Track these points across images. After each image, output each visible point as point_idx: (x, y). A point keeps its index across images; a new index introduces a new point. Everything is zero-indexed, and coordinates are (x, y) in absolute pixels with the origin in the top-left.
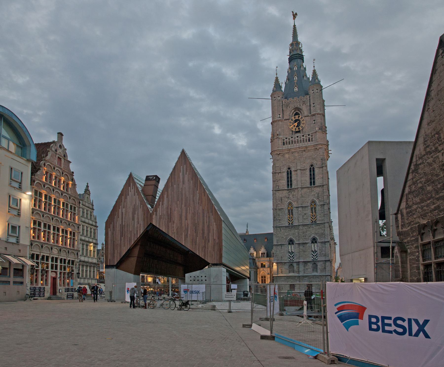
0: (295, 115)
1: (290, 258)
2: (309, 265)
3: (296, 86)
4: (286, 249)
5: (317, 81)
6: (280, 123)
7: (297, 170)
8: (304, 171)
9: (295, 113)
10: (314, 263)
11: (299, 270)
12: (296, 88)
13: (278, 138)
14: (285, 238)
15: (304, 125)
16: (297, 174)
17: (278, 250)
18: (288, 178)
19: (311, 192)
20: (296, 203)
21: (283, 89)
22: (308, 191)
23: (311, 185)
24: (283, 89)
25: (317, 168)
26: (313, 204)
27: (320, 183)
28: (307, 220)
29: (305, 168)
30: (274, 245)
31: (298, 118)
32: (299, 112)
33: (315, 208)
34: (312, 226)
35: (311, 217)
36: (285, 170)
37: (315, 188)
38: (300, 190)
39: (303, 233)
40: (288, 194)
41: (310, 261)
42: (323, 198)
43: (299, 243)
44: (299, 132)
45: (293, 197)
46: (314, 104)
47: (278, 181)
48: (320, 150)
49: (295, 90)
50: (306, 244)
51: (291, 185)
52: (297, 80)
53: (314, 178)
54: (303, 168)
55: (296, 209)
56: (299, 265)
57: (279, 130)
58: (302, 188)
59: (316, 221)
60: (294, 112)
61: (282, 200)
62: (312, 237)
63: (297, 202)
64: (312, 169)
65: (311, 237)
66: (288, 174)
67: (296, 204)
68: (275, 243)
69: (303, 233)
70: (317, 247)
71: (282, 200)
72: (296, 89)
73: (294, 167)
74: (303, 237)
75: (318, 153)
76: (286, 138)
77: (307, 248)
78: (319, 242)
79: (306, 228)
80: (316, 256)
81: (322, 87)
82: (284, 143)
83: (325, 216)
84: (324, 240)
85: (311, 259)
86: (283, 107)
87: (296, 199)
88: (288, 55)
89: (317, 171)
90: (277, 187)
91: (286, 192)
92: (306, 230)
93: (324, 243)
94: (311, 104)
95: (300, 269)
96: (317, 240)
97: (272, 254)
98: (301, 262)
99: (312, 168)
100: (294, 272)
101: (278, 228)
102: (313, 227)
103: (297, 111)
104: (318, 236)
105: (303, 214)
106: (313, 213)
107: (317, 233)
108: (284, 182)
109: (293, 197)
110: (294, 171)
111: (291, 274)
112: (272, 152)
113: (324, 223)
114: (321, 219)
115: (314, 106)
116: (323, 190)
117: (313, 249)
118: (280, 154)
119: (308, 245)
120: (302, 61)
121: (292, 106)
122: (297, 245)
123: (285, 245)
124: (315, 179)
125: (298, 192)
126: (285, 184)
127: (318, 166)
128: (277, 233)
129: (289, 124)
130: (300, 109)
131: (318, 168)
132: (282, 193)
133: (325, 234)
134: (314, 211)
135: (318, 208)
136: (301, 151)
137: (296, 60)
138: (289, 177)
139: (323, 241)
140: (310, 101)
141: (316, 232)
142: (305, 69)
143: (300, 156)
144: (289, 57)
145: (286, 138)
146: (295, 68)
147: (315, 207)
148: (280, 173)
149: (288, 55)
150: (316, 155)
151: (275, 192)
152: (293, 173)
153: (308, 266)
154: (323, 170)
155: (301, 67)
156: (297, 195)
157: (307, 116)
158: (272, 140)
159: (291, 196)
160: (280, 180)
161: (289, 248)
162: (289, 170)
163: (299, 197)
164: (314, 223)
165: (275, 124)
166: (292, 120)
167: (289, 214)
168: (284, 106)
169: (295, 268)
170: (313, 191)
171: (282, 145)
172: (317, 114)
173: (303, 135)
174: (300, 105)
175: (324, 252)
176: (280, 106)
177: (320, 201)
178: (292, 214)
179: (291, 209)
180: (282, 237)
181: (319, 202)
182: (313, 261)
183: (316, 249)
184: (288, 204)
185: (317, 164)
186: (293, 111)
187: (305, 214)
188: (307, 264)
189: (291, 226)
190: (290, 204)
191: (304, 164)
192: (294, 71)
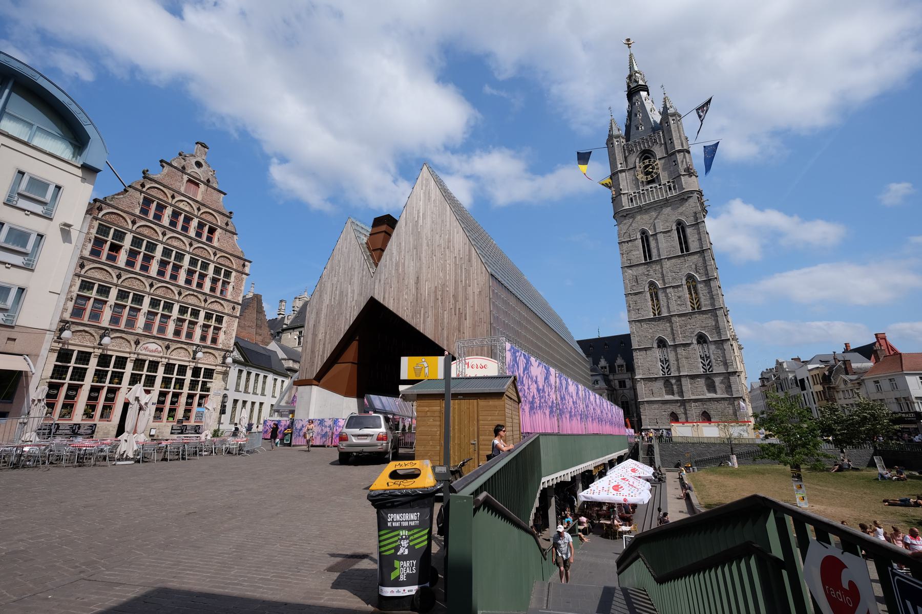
0: (644, 159)
9: (643, 157)
22: (679, 261)
23: (682, 251)
31: (649, 162)
32: (650, 155)
39: (681, 328)
44: (652, 181)
45: (656, 274)
62: (697, 334)
63: (664, 280)
80: (708, 365)
87: (660, 275)
89: (689, 231)
93: (720, 342)
96: (706, 338)
98: (684, 375)
102: (696, 317)
103: (646, 155)
108: (638, 254)
110: (652, 235)
118: (628, 216)
119: (692, 346)
122: (672, 347)
135: (700, 287)
141: (704, 325)
145: (634, 193)
147: (695, 285)
148: (630, 241)
152: (651, 239)
159: (652, 272)
162: (644, 236)
164: (697, 310)
179: (654, 292)
181: (699, 277)
186: (640, 155)
187: (679, 297)
189: (658, 318)
190: (652, 284)
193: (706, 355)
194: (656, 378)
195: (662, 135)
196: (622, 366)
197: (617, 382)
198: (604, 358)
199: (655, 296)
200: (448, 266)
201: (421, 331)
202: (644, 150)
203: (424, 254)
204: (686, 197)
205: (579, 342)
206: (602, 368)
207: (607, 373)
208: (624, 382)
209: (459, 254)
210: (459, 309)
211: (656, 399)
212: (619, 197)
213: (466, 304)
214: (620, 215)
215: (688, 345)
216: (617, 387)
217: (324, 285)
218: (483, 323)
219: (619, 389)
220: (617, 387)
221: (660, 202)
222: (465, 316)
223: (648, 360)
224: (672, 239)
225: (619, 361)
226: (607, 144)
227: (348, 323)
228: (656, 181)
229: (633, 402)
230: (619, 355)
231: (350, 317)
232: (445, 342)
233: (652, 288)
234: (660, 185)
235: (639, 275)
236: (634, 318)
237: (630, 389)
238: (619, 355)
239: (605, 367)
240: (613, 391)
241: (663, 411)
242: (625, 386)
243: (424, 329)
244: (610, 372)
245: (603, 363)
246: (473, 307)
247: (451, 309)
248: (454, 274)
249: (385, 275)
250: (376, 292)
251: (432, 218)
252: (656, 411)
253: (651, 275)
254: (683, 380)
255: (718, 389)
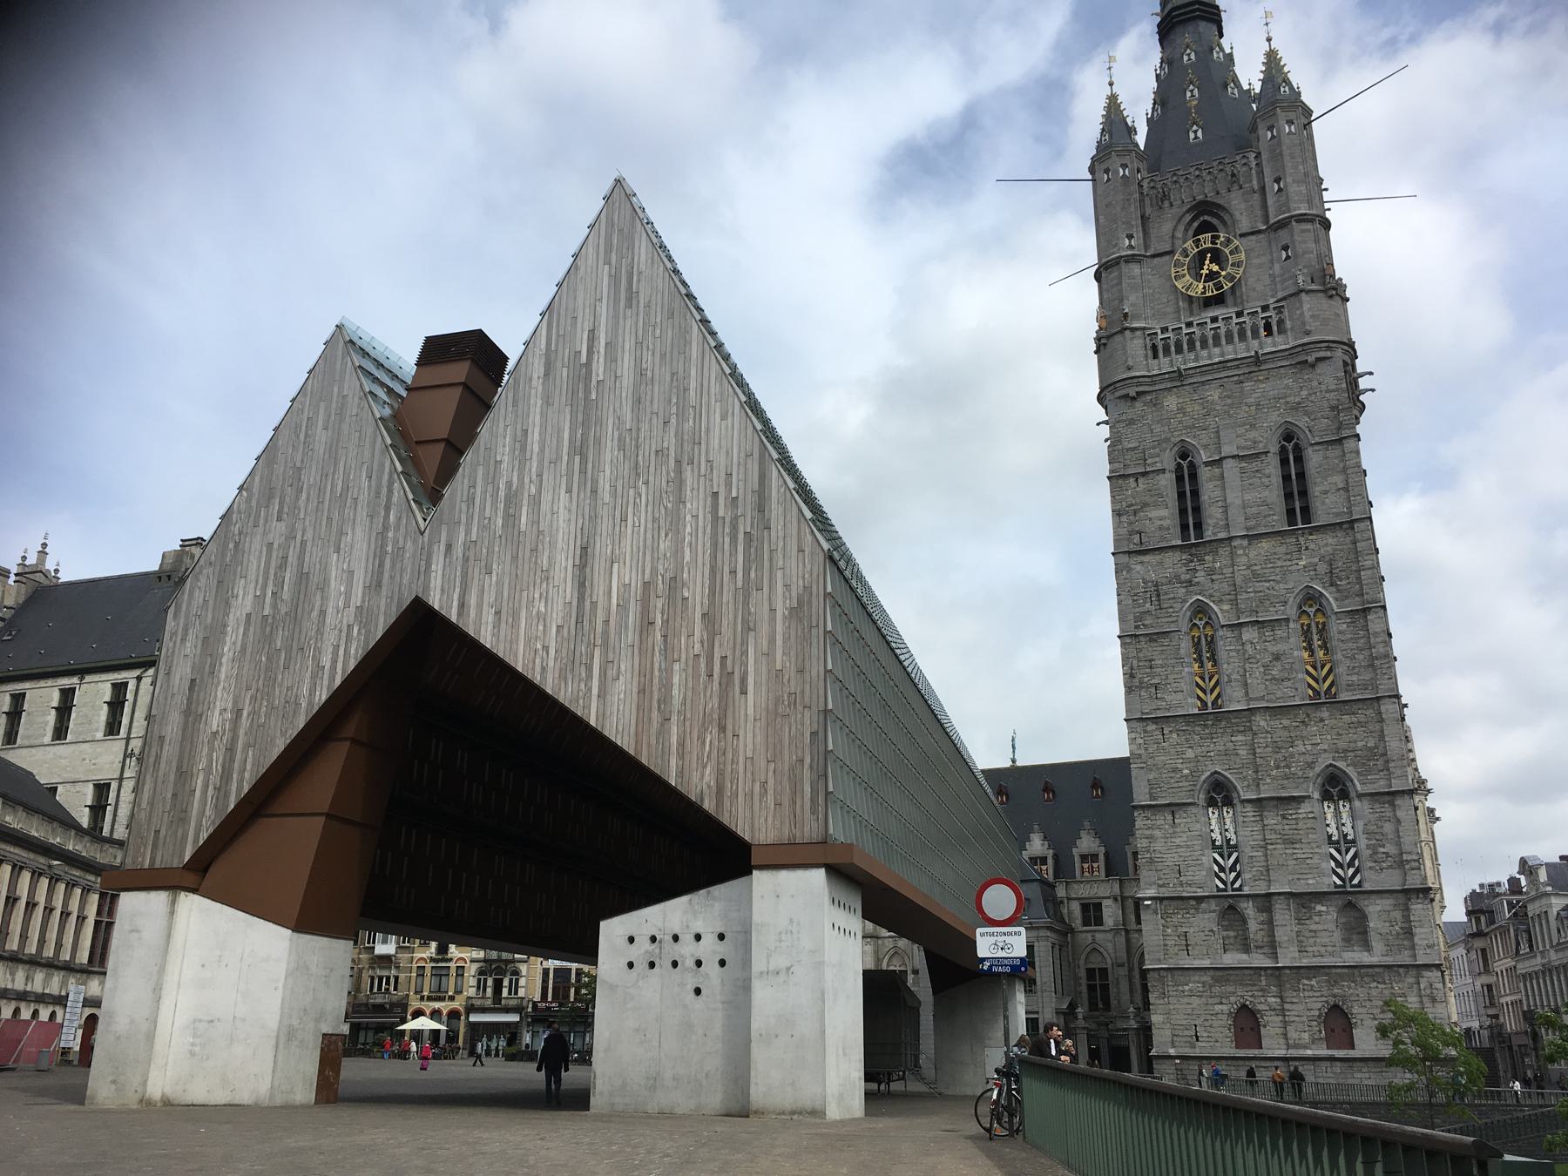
0: (1197, 233)
1: (1222, 875)
2: (1320, 914)
3: (1194, 123)
4: (1198, 826)
5: (1287, 89)
6: (1135, 269)
7: (1221, 459)
8: (1256, 465)
9: (1196, 224)
10: (1349, 901)
11: (1272, 934)
12: (1195, 128)
13: (1126, 329)
14: (1186, 771)
15: (1242, 270)
16: (1222, 477)
17: (1157, 833)
18: (1181, 495)
19: (1295, 555)
20: (1226, 607)
21: (1141, 139)
22: (1283, 549)
23: (1292, 521)
24: (1141, 139)
25: (1312, 445)
26: (1311, 611)
27: (1337, 515)
28: (1289, 684)
29: (1260, 448)
30: (1135, 807)
31: (1213, 243)
32: (1215, 221)
33: (1323, 630)
34: (1318, 714)
35: (1308, 673)
36: (1168, 460)
37: (1311, 534)
38: (1244, 549)
39: (1278, 749)
40: (1185, 565)
41: (1325, 893)
42: (1359, 578)
43: (1260, 800)
44: (1219, 300)
46: (1278, 180)
47: (1135, 512)
48: (1321, 368)
49: (1192, 136)
50: (1294, 805)
51: (1199, 526)
52: (1200, 100)
53: (1304, 493)
54: (1249, 448)
55: (1229, 634)
56: (1268, 910)
57: (1132, 298)
58: (1253, 538)
59: (1333, 690)
60: (1193, 220)
61: (1158, 595)
62: (1323, 770)
63: (1234, 603)
64: (1291, 451)
65: (1318, 769)
66: (1180, 479)
67: (1227, 611)
68: (1141, 796)
69: (1278, 749)
70: (1353, 818)
71: (1158, 595)
72: (1196, 134)
73: (1206, 447)
74: (1278, 767)
75: (1315, 383)
76: (1165, 330)
77: (1301, 825)
78: (1360, 796)
79: (1286, 722)
80: (1351, 864)
81: (1308, 112)
82: (1154, 348)
83: (1377, 663)
84: (1382, 782)
85: (1326, 881)
86: (1142, 207)
87: (1226, 587)
88: (1157, 14)
89: (1314, 459)
90: (1136, 538)
91: (1177, 556)
92: (1287, 734)
93: (1387, 798)
94: (1268, 180)
95: (1281, 934)
96: (1348, 784)
97: (1129, 855)
98: (1280, 894)
99: (1290, 447)
100: (1246, 949)
101: (1151, 727)
102: (1322, 720)
103: (1206, 218)
104: (1354, 765)
105: (1267, 659)
106: (1312, 653)
107: (1345, 751)
108: (1163, 517)
109: (1212, 580)
110: (1207, 464)
111: (1232, 959)
112: (1105, 392)
113: (1378, 699)
114: (1355, 678)
115: (1280, 190)
116: (1355, 542)
117: (1332, 830)
118: (1143, 398)
119: (1305, 808)
120: (1215, 28)
121: (1183, 197)
122: (1249, 808)
123: (1193, 810)
124: (1310, 492)
125: (1232, 555)
126: (1166, 523)
127: (1317, 439)
128: (1146, 749)
129: (1173, 270)
130: (1219, 206)
131: (1317, 448)
132: (1161, 563)
133: (1385, 754)
134: (1317, 643)
135: (1337, 627)
136: (1236, 378)
137: (1191, 27)
138: (1188, 494)
139: (1381, 786)
140: (1261, 173)
141: (1341, 745)
142: (1230, 58)
143: (1229, 401)
144: (1159, 19)
145: (1165, 330)
146: (1189, 57)
147: (1324, 624)
148: (1144, 474)
149: (1157, 14)
150: (1304, 393)
151: (1125, 558)
152: (1204, 473)
153: (1316, 919)
154: (1344, 455)
155: (1212, 50)
156: (1228, 571)
157: (1252, 233)
158: (1103, 341)
159: (1201, 577)
160: (1146, 505)
161: (1213, 822)
162: (1185, 464)
163: (1239, 580)
164: (1326, 699)
165: (1113, 275)
166: (1185, 253)
167: (1200, 660)
168: (1147, 201)
169: (1253, 926)
170: (1307, 549)
171: (1146, 357)
172: (1298, 221)
173: (1236, 309)
174: (1218, 193)
175: (1390, 848)
176: (1130, 205)
177: (1342, 596)
178: (1215, 661)
179: (1206, 636)
180: (1175, 770)
181: (1336, 599)
182: (1339, 892)
183: (1348, 829)
184: (1189, 613)
185: (1312, 427)
186: (1188, 217)
187: (1277, 657)
188: (1310, 909)
189: (1212, 717)
190: (1200, 610)
191: (1253, 434)
192: (1185, 68)
193: (1345, 836)
194: (1200, 899)
195: (1253, 164)
196: (1094, 857)
197: (1076, 907)
198: (1042, 830)
199: (1206, 650)
200: (688, 518)
201: (593, 723)
202: (1202, 203)
203: (608, 472)
204: (1311, 359)
205: (983, 771)
206: (1033, 860)
207: (1050, 877)
208: (1098, 907)
209: (729, 485)
210: (724, 658)
211: (1197, 963)
212: (1118, 338)
213: (745, 643)
214: (1118, 394)
215: (1299, 800)
216: (1077, 923)
217: (237, 544)
218: (800, 708)
219: (1081, 928)
220: (1077, 923)
221: (1237, 367)
222: (744, 681)
223: (1178, 841)
224: (1265, 480)
225: (1087, 843)
226: (1092, 170)
227: (326, 683)
228: (1229, 300)
229: (1123, 971)
230: (1087, 824)
231: (334, 662)
232: (673, 762)
233: (1201, 624)
234: (1239, 314)
235: (1164, 580)
236: (1148, 708)
237: (1115, 931)
238: (1087, 824)
239: (1044, 860)
240: (1066, 935)
241: (1217, 1000)
242: (1099, 922)
243: (602, 715)
244: (1056, 876)
245: (1037, 845)
246: (769, 655)
247: (697, 656)
248: (708, 545)
249: (468, 532)
250: (436, 582)
251: (638, 361)
252: (1196, 1001)
253: (1198, 583)
254: (1279, 907)
255: (1373, 936)
